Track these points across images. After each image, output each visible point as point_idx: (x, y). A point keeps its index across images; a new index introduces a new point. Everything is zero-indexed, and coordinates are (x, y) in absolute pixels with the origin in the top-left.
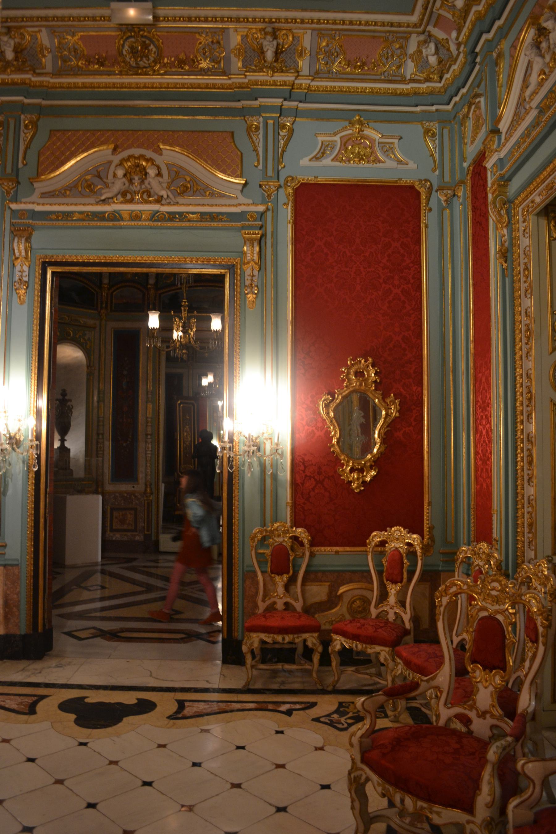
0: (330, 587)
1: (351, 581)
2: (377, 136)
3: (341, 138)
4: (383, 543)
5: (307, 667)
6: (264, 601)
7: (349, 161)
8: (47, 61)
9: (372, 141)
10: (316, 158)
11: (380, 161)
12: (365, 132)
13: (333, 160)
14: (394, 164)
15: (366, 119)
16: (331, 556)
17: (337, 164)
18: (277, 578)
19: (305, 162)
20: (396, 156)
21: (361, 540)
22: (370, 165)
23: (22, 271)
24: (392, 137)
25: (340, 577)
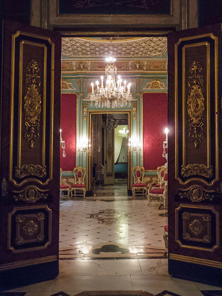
0: (151, 178)
1: (155, 177)
2: (159, 82)
3: (152, 83)
4: (160, 169)
5: (145, 194)
6: (135, 182)
7: (154, 88)
8: (89, 68)
9: (158, 83)
10: (146, 88)
11: (160, 88)
12: (157, 82)
13: (150, 88)
14: (163, 89)
15: (157, 78)
16: (150, 172)
17: (151, 89)
18: (138, 177)
19: (144, 89)
20: (163, 86)
21: (156, 169)
22: (158, 89)
23: (85, 114)
24: (163, 82)
25: (152, 176)
